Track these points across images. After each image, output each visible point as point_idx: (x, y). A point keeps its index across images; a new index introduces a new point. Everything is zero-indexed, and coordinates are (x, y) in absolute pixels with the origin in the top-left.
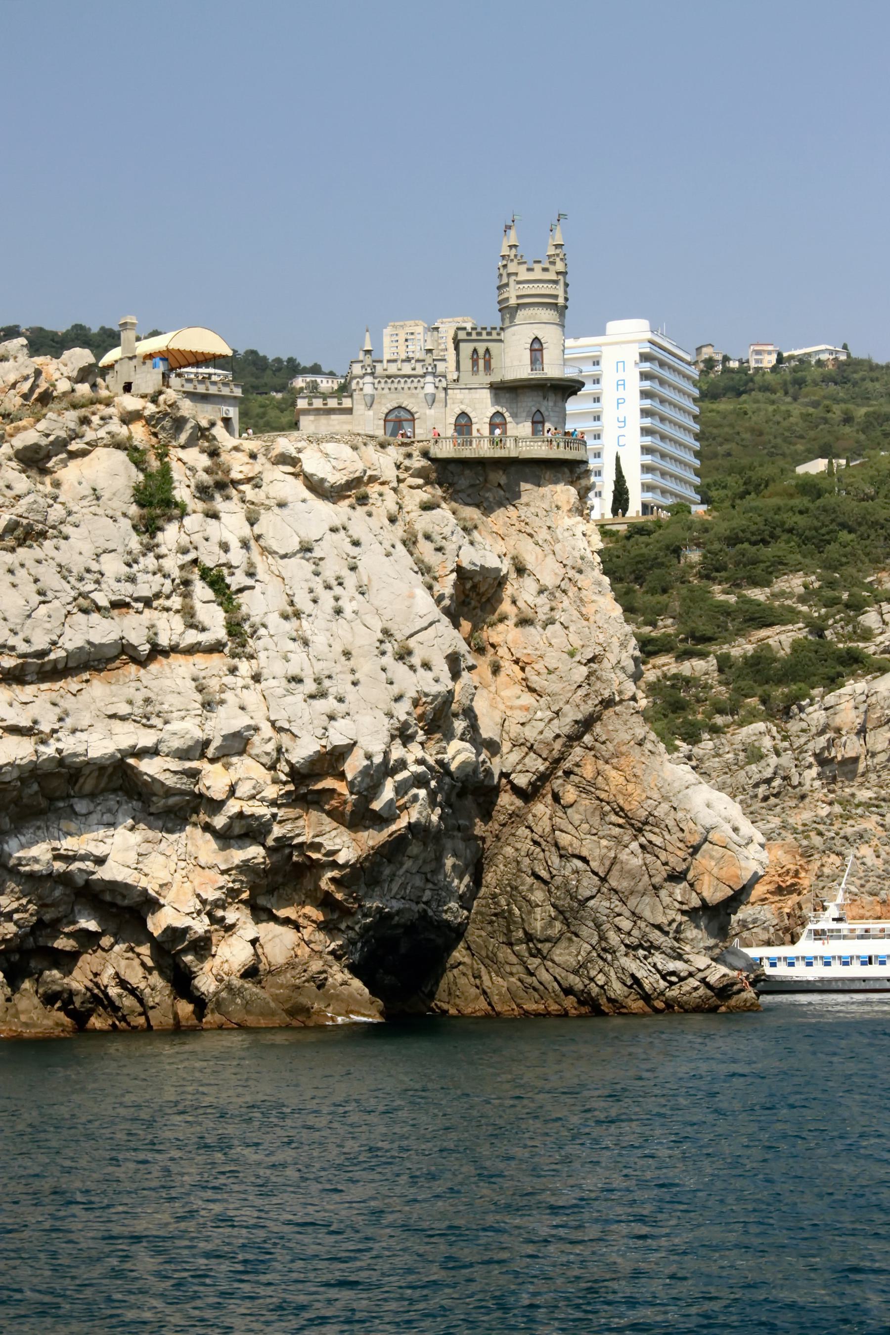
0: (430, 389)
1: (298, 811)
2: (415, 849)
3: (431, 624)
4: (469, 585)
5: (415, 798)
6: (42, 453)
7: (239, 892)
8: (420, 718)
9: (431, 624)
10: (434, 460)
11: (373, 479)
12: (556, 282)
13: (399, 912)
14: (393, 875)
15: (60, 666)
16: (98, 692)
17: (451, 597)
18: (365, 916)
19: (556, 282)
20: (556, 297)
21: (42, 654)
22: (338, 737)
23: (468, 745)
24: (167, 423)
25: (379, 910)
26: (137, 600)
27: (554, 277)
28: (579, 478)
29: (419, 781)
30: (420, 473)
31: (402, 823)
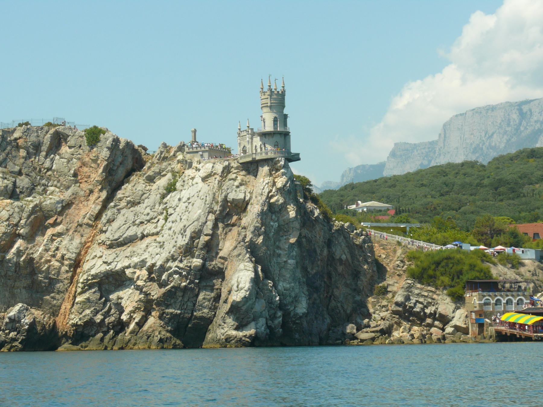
0: (248, 139)
1: (151, 283)
2: (180, 294)
3: (193, 222)
4: (233, 205)
5: (174, 279)
6: (153, 178)
7: (140, 308)
8: (181, 253)
9: (193, 222)
10: (240, 163)
11: (215, 174)
12: (267, 98)
13: (180, 314)
14: (175, 302)
15: (123, 243)
16: (128, 250)
17: (220, 210)
18: (167, 315)
19: (267, 98)
20: (267, 103)
21: (116, 240)
22: (153, 262)
23: (199, 260)
24: (184, 162)
25: (172, 313)
26: (146, 220)
27: (267, 97)
28: (276, 164)
29: (176, 272)
30: (237, 168)
31: (169, 286)
